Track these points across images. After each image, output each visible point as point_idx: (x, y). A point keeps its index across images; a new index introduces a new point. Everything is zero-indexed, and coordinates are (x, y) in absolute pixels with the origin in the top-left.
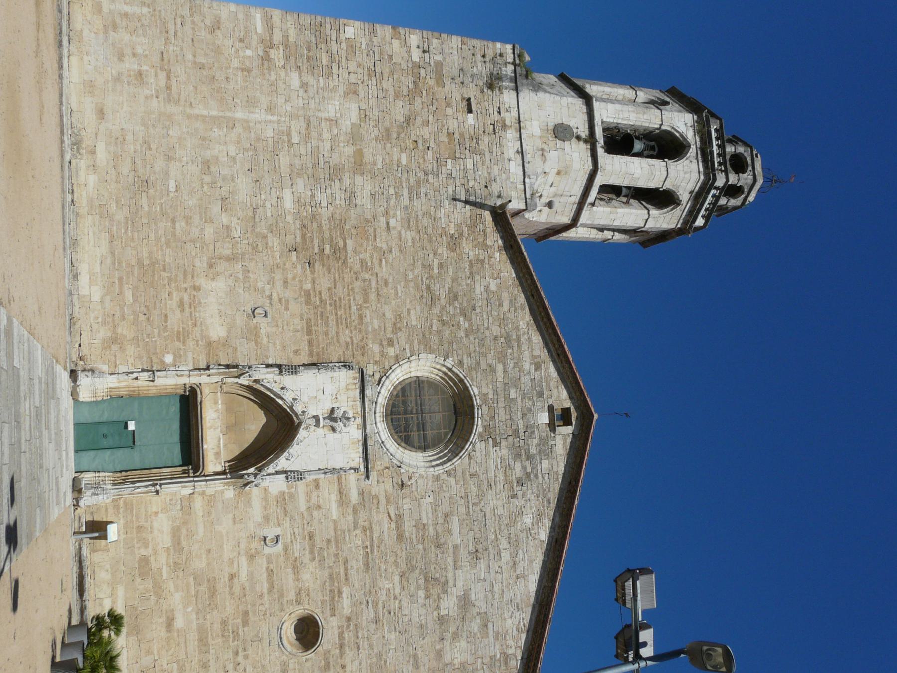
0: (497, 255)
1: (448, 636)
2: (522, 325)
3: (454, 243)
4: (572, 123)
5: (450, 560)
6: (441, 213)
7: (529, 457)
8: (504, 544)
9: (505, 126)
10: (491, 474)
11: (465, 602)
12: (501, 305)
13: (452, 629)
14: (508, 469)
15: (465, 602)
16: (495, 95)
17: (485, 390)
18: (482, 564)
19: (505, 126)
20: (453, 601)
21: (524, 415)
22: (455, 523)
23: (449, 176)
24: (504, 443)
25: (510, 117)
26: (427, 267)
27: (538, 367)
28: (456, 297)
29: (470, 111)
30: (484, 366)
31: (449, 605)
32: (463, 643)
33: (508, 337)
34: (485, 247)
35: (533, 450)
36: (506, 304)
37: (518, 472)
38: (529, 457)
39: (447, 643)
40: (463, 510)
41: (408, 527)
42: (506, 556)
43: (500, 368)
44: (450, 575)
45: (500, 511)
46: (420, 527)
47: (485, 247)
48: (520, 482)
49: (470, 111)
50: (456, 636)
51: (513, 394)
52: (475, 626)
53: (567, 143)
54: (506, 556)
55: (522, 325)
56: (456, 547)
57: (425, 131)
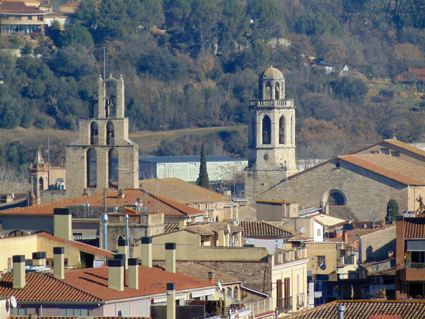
0: (299, 180)
1: (383, 200)
2: (315, 174)
3: (296, 191)
4: (264, 154)
5: (368, 198)
6: (289, 194)
7: (347, 175)
8: (365, 184)
9: (266, 175)
10: (349, 186)
11: (377, 195)
12: (311, 180)
13: (382, 199)
14: (349, 182)
15: (377, 195)
16: (259, 177)
17: (331, 186)
18: (370, 190)
19: (266, 175)
20: (376, 198)
21: (337, 176)
22: (360, 196)
23: (280, 191)
24: (343, 182)
25: (264, 173)
26: (302, 198)
27: (326, 171)
28: (309, 192)
29: (263, 184)
30: (325, 186)
31: (377, 199)
32: (386, 197)
33: (319, 178)
34: (297, 183)
35: (345, 174)
36: (311, 178)
37: (349, 179)
38: (347, 175)
39: (385, 200)
40: (357, 194)
41: (359, 208)
42: (368, 184)
43: (326, 181)
44: (371, 198)
45: (358, 184)
46: (359, 205)
47: (297, 183)
48: (352, 179)
49: (263, 184)
50: (384, 198)
51: (332, 178)
52: (383, 193)
53: (270, 156)
54: (368, 184)
55: (315, 174)
56: (365, 197)
57: (270, 197)
